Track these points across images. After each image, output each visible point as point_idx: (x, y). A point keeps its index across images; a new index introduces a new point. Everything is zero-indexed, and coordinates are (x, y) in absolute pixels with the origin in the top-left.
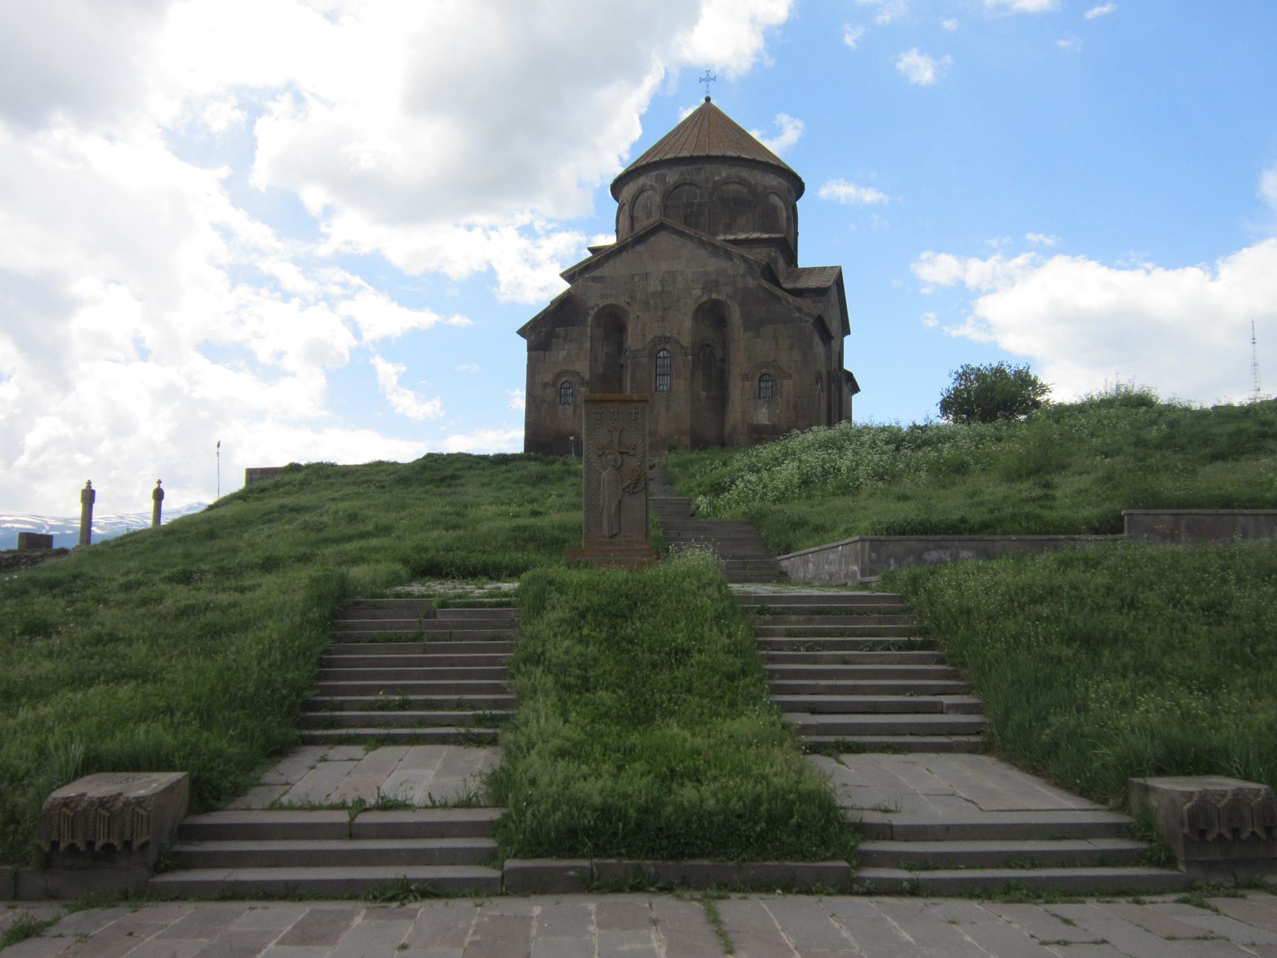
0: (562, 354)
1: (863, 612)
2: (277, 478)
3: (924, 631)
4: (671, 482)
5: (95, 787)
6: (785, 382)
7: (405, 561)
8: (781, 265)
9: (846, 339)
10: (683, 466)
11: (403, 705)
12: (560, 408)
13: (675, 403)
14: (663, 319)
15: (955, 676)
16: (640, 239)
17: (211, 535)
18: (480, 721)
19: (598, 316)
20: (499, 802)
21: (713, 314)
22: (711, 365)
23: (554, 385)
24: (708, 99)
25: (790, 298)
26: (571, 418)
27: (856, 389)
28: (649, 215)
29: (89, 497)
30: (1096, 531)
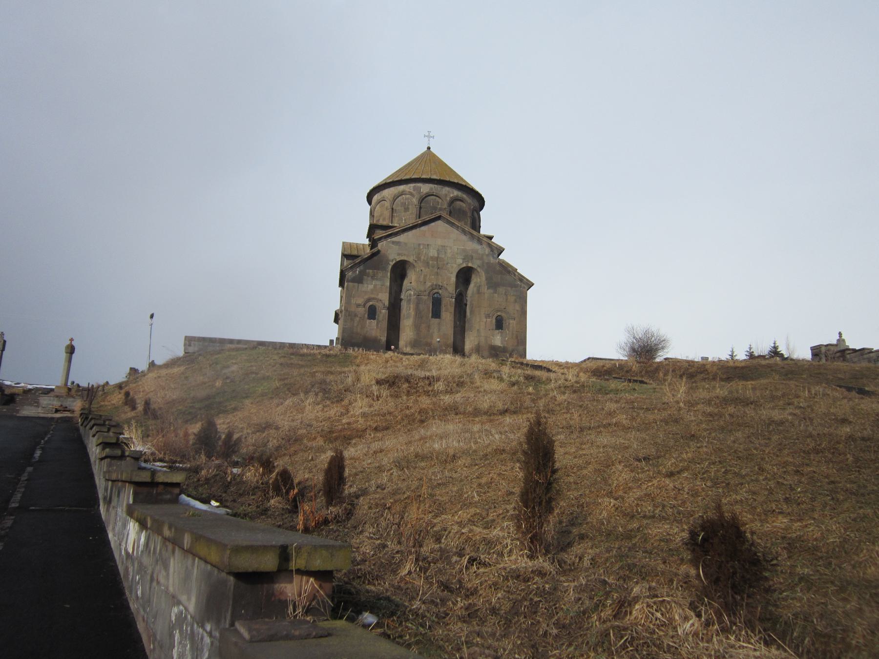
0: (371, 287)
12: (368, 321)
14: (437, 274)
19: (394, 266)
23: (364, 306)
24: (429, 148)
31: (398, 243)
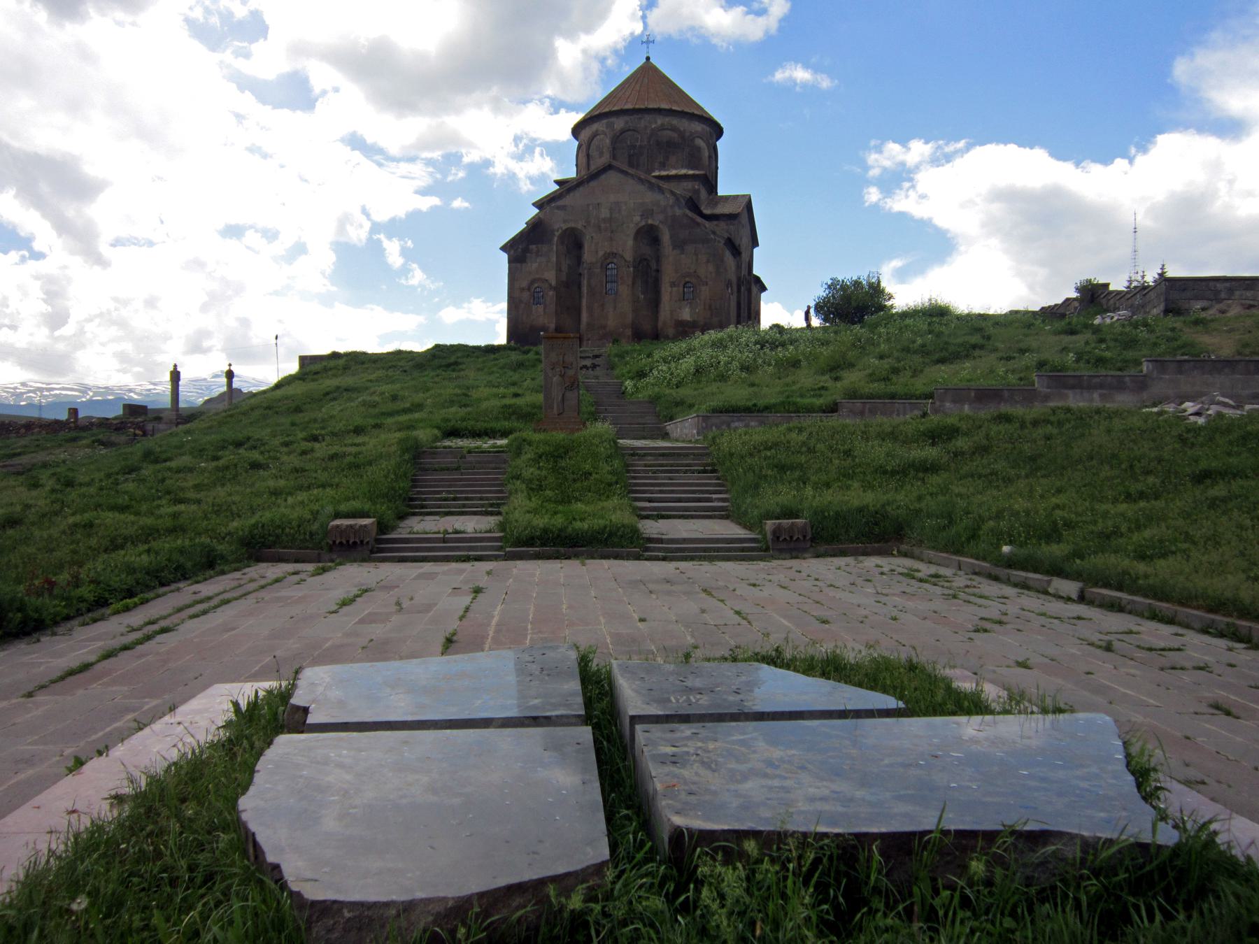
0: (535, 265)
1: (687, 455)
2: (324, 363)
3: (713, 464)
4: (612, 367)
5: (337, 522)
6: (703, 288)
7: (438, 428)
8: (703, 194)
9: (756, 250)
10: (621, 356)
11: (455, 499)
12: (534, 307)
13: (620, 306)
14: (611, 239)
15: (723, 485)
16: (593, 176)
17: (298, 410)
18: (492, 505)
19: (561, 237)
20: (503, 530)
21: (649, 235)
22: (648, 275)
23: (529, 289)
24: (648, 59)
25: (707, 224)
26: (543, 316)
27: (764, 289)
28: (601, 154)
29: (175, 376)
30: (824, 412)
31: (563, 208)
